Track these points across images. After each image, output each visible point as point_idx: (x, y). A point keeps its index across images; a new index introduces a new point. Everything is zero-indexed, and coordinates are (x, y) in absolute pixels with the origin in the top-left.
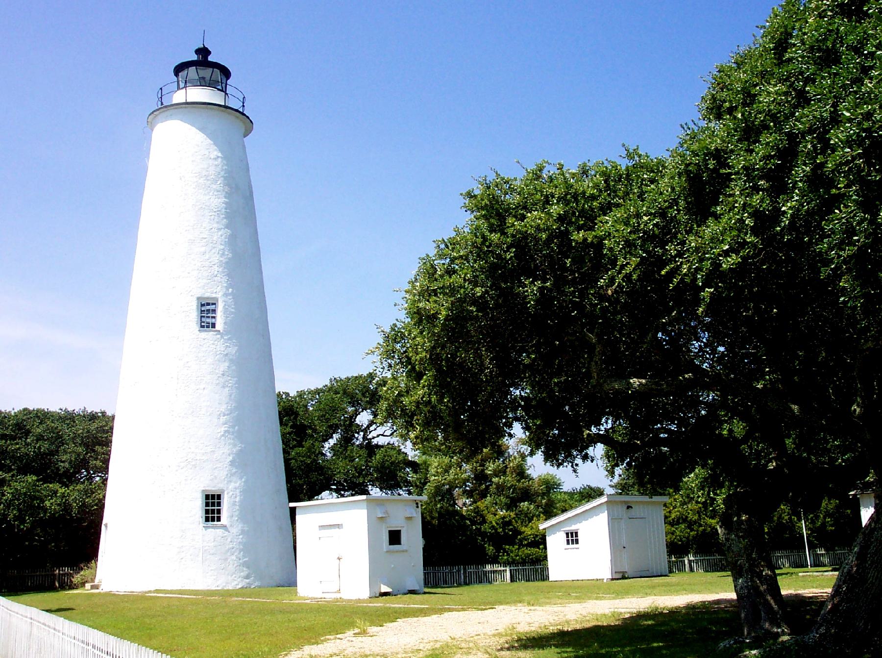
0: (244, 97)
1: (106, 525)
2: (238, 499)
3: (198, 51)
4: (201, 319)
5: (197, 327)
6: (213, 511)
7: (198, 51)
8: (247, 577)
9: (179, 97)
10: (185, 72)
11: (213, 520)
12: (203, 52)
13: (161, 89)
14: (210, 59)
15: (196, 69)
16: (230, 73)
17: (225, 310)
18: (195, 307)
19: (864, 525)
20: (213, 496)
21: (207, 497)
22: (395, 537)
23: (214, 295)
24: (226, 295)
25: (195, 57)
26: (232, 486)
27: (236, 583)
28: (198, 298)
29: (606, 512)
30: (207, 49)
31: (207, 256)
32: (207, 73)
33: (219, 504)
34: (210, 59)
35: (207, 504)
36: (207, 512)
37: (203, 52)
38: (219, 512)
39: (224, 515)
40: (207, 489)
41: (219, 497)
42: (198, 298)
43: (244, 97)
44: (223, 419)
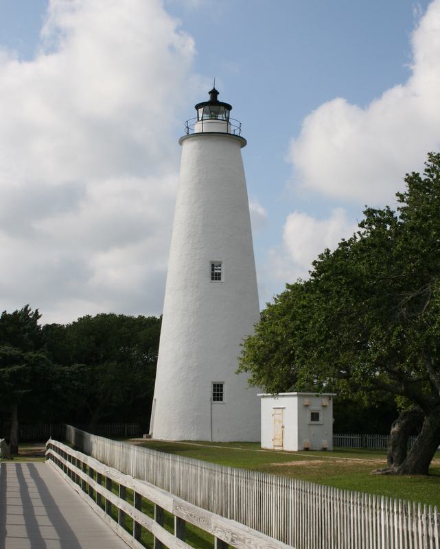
4: (213, 270)
5: (210, 280)
6: (218, 394)
12: (214, 93)
20: (218, 385)
21: (214, 385)
22: (315, 417)
23: (220, 260)
28: (211, 262)
32: (215, 108)
33: (222, 390)
35: (214, 390)
36: (214, 394)
37: (214, 93)
38: (222, 395)
41: (222, 386)
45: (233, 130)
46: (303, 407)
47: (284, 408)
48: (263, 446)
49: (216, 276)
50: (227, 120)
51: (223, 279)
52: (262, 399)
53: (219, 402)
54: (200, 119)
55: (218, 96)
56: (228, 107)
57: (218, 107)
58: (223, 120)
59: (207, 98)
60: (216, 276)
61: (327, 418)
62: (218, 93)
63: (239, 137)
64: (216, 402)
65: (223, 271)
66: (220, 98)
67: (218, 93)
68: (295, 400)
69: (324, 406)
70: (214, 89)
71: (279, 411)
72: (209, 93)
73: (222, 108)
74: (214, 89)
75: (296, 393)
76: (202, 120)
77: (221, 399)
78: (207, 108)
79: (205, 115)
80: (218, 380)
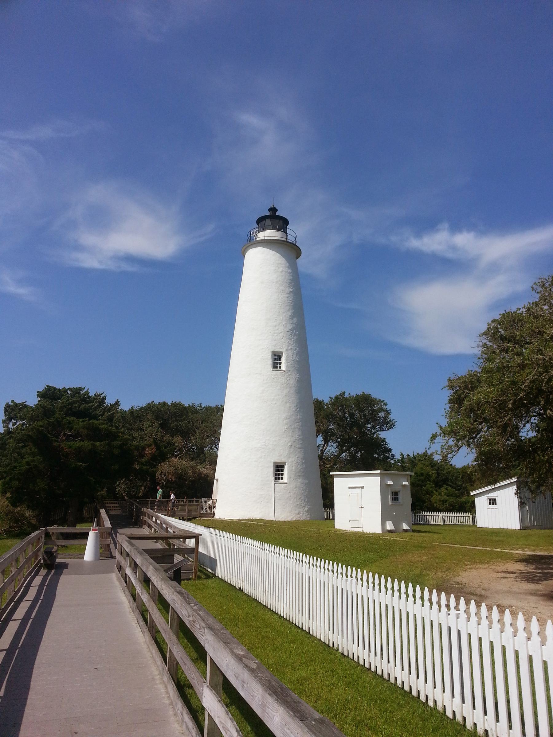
1: (217, 480)
2: (294, 468)
3: (270, 210)
7: (270, 210)
8: (299, 513)
9: (261, 236)
10: (263, 222)
14: (277, 214)
17: (287, 360)
18: (270, 356)
21: (276, 466)
22: (395, 496)
23: (281, 350)
24: (287, 350)
25: (268, 213)
26: (290, 460)
27: (292, 517)
29: (516, 486)
30: (275, 208)
31: (277, 328)
34: (277, 214)
36: (276, 474)
37: (273, 210)
38: (282, 474)
39: (285, 477)
40: (276, 461)
44: (285, 422)
45: (291, 239)
46: (384, 487)
47: (364, 487)
52: (336, 480)
53: (281, 481)
57: (278, 221)
68: (377, 479)
75: (379, 471)
80: (279, 460)
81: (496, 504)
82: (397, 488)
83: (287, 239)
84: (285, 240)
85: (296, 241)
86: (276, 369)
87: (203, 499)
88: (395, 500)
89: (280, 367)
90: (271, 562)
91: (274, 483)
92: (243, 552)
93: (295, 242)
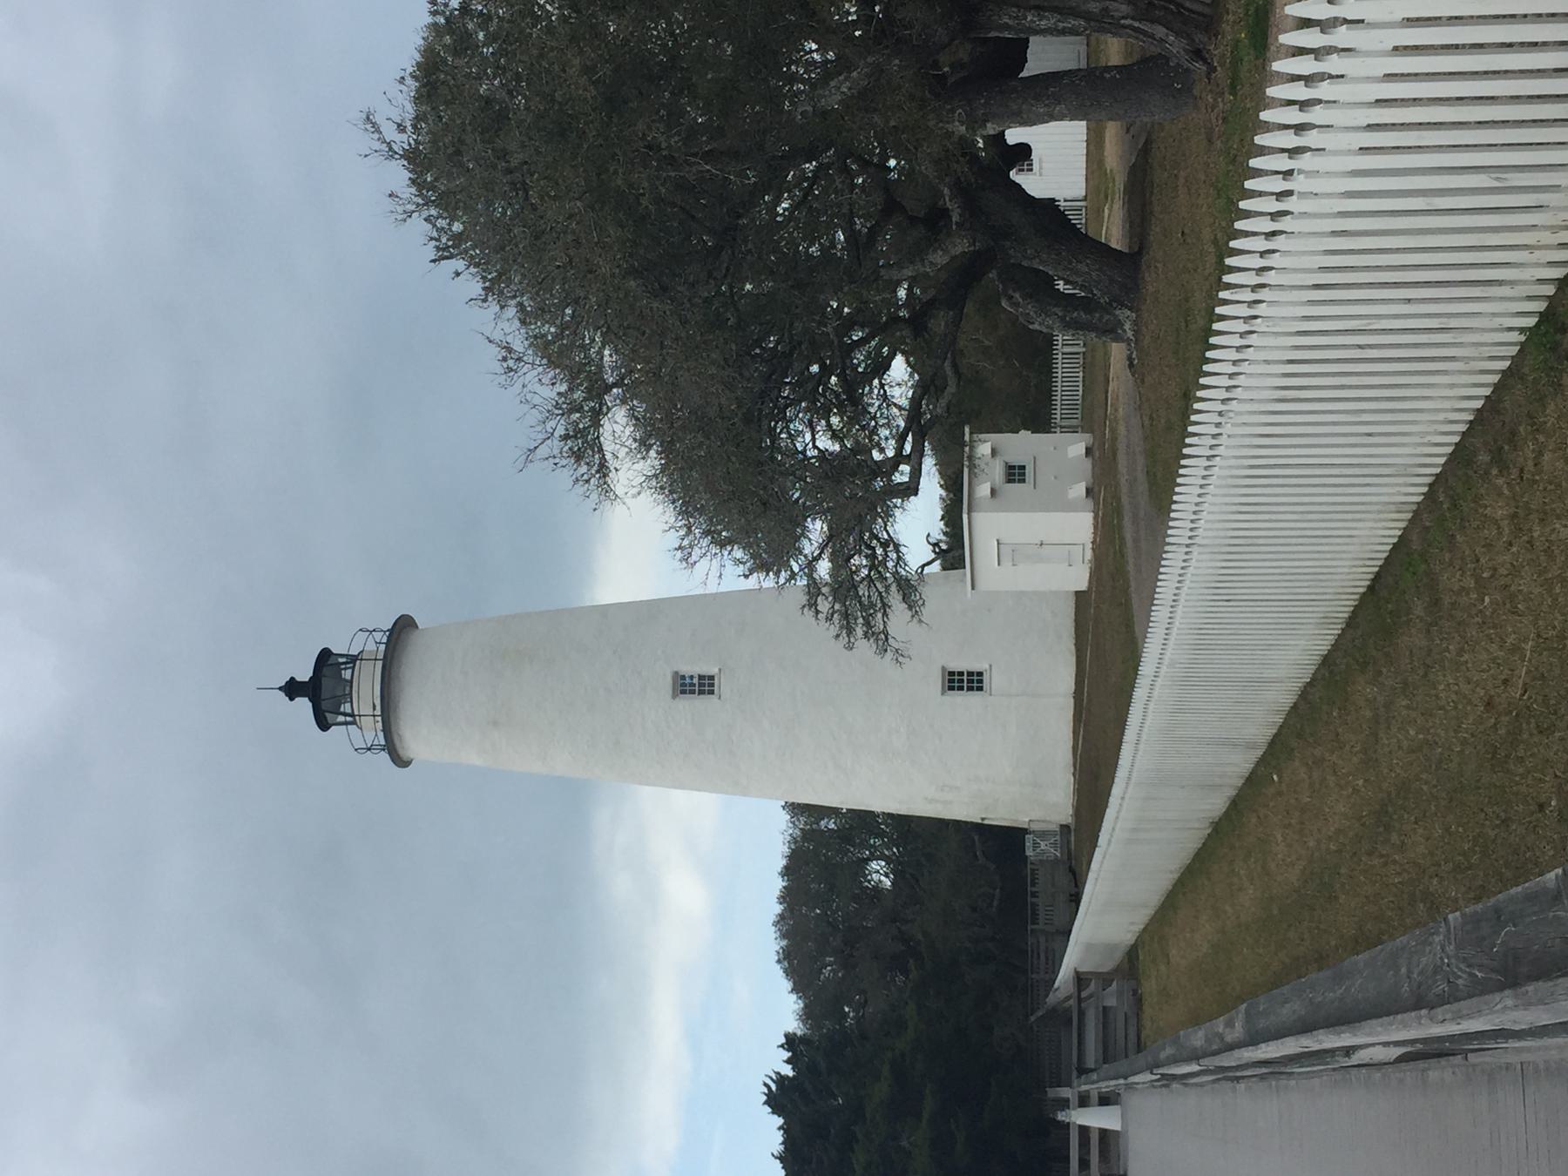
0: (361, 630)
1: (983, 819)
11: (981, 681)
12: (292, 689)
13: (356, 750)
15: (324, 700)
16: (323, 650)
19: (1021, 76)
20: (950, 681)
21: (951, 688)
22: (1015, 474)
28: (674, 696)
30: (287, 683)
32: (327, 684)
33: (961, 674)
35: (961, 688)
36: (970, 689)
37: (292, 689)
38: (970, 674)
41: (951, 673)
42: (674, 696)
43: (361, 630)
45: (373, 646)
47: (998, 541)
48: (1083, 586)
49: (704, 686)
50: (353, 660)
51: (714, 671)
53: (986, 678)
54: (349, 719)
55: (298, 679)
56: (325, 656)
58: (353, 668)
59: (304, 705)
60: (704, 686)
61: (1021, 445)
62: (292, 679)
63: (391, 631)
64: (986, 685)
65: (693, 669)
66: (304, 674)
67: (292, 679)
69: (994, 452)
70: (280, 689)
71: (1005, 550)
72: (292, 699)
73: (326, 671)
74: (280, 689)
76: (352, 715)
77: (980, 674)
78: (325, 705)
79: (342, 709)
80: (936, 682)
81: (1023, 467)
82: (997, 471)
83: (376, 659)
84: (379, 664)
85: (374, 630)
86: (716, 689)
87: (1029, 852)
88: (1024, 474)
89: (711, 678)
90: (1230, 545)
91: (991, 695)
92: (1201, 597)
93: (378, 636)
